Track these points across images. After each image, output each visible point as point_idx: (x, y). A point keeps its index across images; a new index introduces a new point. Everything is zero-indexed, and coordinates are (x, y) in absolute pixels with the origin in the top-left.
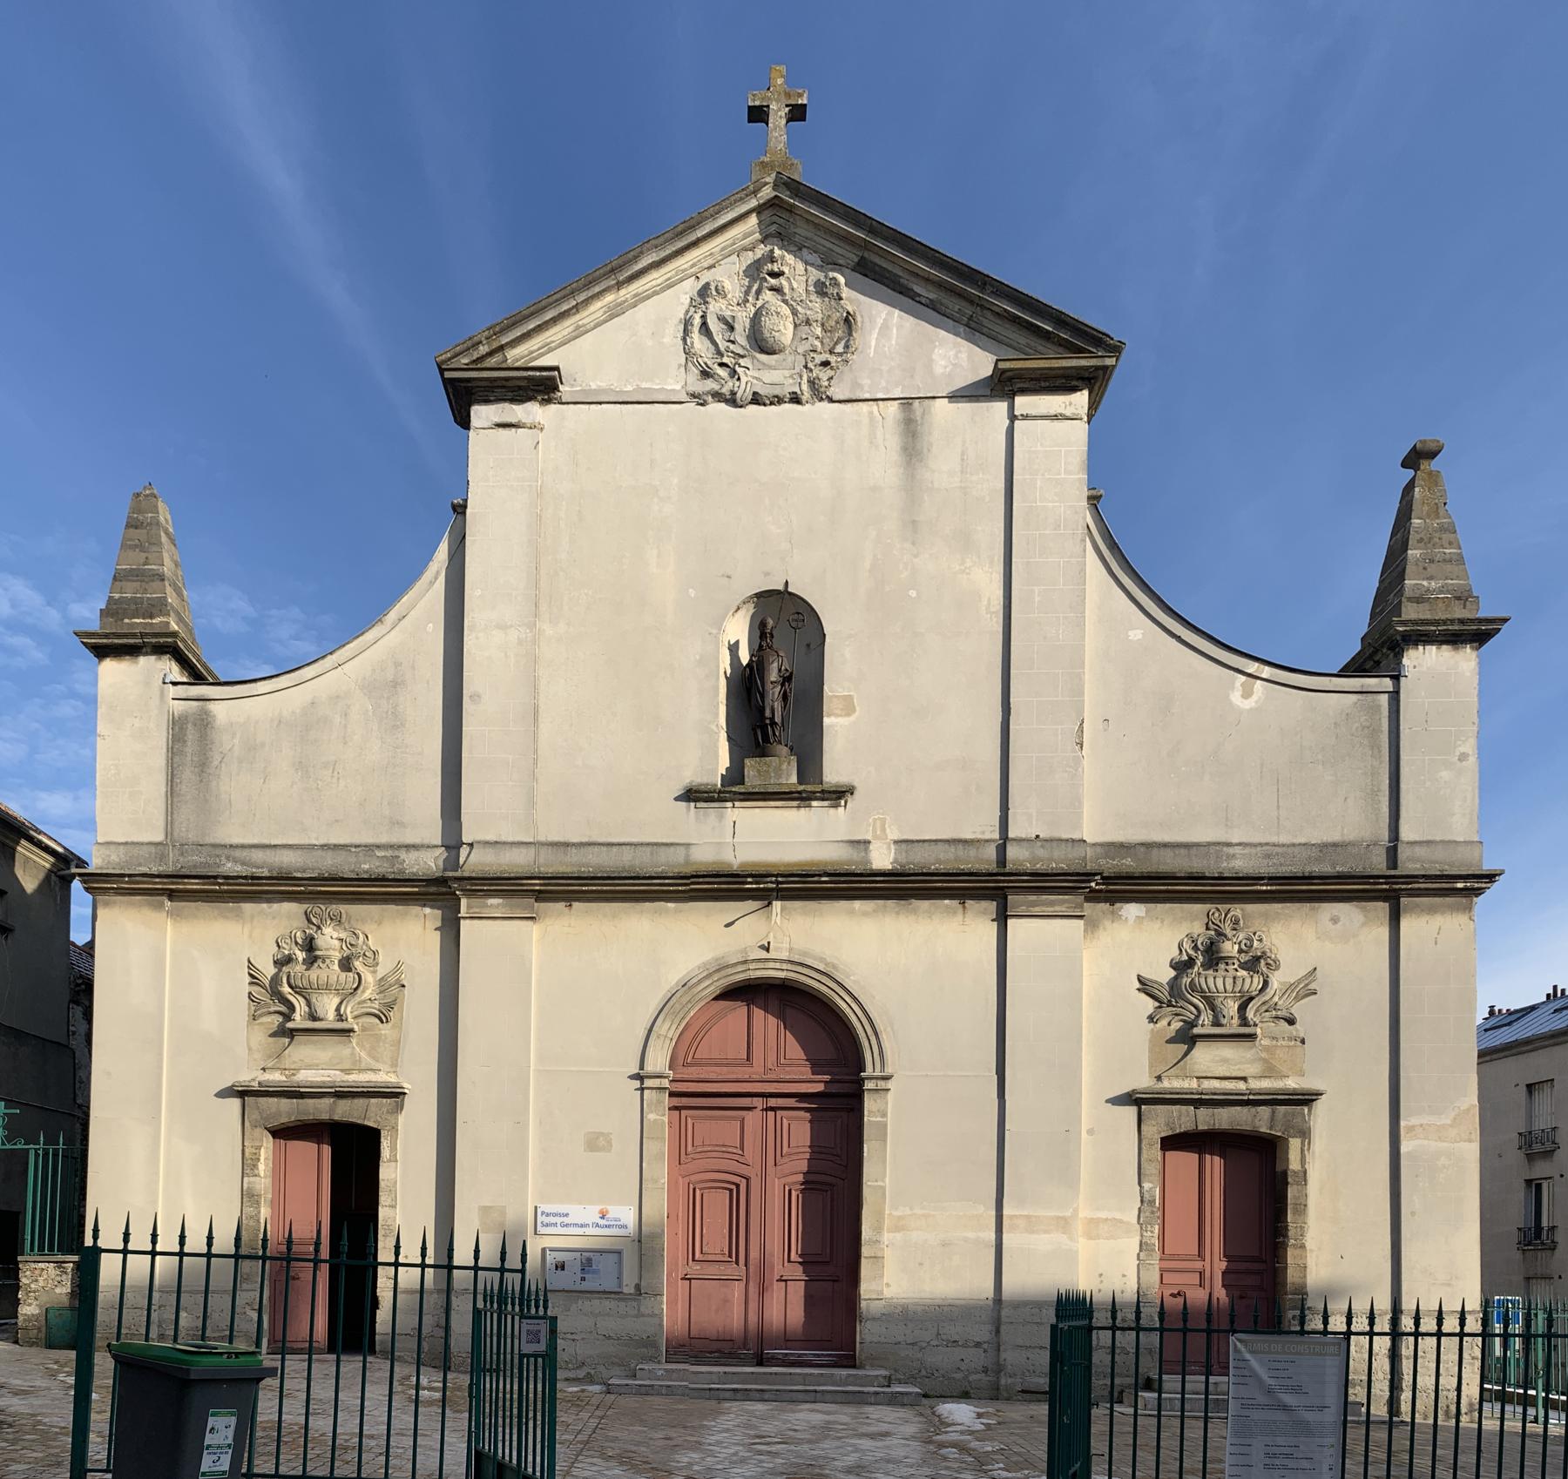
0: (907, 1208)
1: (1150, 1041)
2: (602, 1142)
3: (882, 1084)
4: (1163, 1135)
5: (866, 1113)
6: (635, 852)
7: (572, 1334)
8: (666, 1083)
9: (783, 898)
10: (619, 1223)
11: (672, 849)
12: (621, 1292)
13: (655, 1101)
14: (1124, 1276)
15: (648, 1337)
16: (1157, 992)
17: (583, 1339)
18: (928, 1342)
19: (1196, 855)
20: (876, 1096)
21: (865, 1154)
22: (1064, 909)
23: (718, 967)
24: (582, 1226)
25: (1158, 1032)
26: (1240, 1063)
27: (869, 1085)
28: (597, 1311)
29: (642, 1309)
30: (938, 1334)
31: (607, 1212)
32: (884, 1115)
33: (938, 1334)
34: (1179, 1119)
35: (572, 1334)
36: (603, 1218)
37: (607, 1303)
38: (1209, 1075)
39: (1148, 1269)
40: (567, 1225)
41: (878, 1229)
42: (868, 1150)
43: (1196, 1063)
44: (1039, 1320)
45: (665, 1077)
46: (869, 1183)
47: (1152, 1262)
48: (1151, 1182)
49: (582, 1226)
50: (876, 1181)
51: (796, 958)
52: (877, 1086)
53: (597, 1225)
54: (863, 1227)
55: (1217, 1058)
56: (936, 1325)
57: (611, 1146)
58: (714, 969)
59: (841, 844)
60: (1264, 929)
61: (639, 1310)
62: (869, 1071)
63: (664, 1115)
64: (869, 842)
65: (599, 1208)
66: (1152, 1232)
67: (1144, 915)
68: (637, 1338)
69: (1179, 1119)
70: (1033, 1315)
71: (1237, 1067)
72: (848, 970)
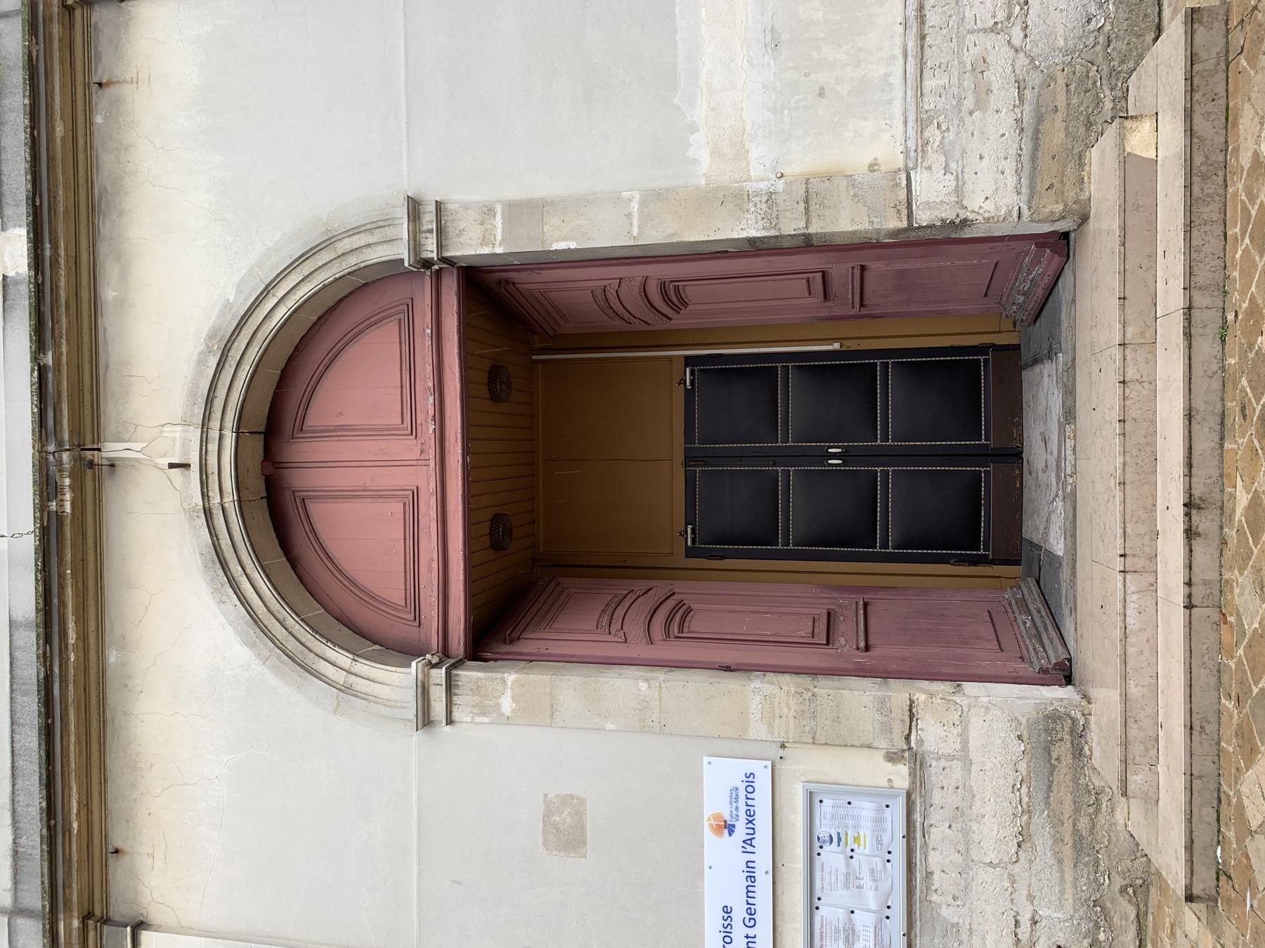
0: (692, 139)
2: (564, 818)
3: (428, 220)
5: (486, 250)
6: (24, 725)
7: (1017, 924)
8: (439, 675)
9: (97, 438)
10: (742, 793)
11: (17, 654)
12: (909, 795)
13: (476, 699)
15: (1019, 737)
17: (1031, 898)
18: (1016, 51)
20: (451, 232)
21: (573, 245)
23: (218, 565)
24: (751, 878)
27: (430, 249)
28: (958, 859)
29: (946, 749)
30: (994, 29)
31: (717, 817)
32: (489, 211)
33: (994, 29)
35: (1017, 924)
36: (731, 829)
37: (936, 835)
40: (751, 912)
41: (738, 199)
42: (566, 239)
45: (427, 676)
46: (635, 232)
49: (751, 878)
50: (629, 215)
51: (199, 411)
52: (431, 231)
53: (749, 842)
54: (735, 236)
56: (970, 38)
57: (572, 796)
58: (221, 573)
59: (9, 331)
61: (950, 758)
62: (401, 252)
63: (504, 681)
64: (5, 277)
65: (708, 834)
68: (1023, 766)
72: (219, 306)
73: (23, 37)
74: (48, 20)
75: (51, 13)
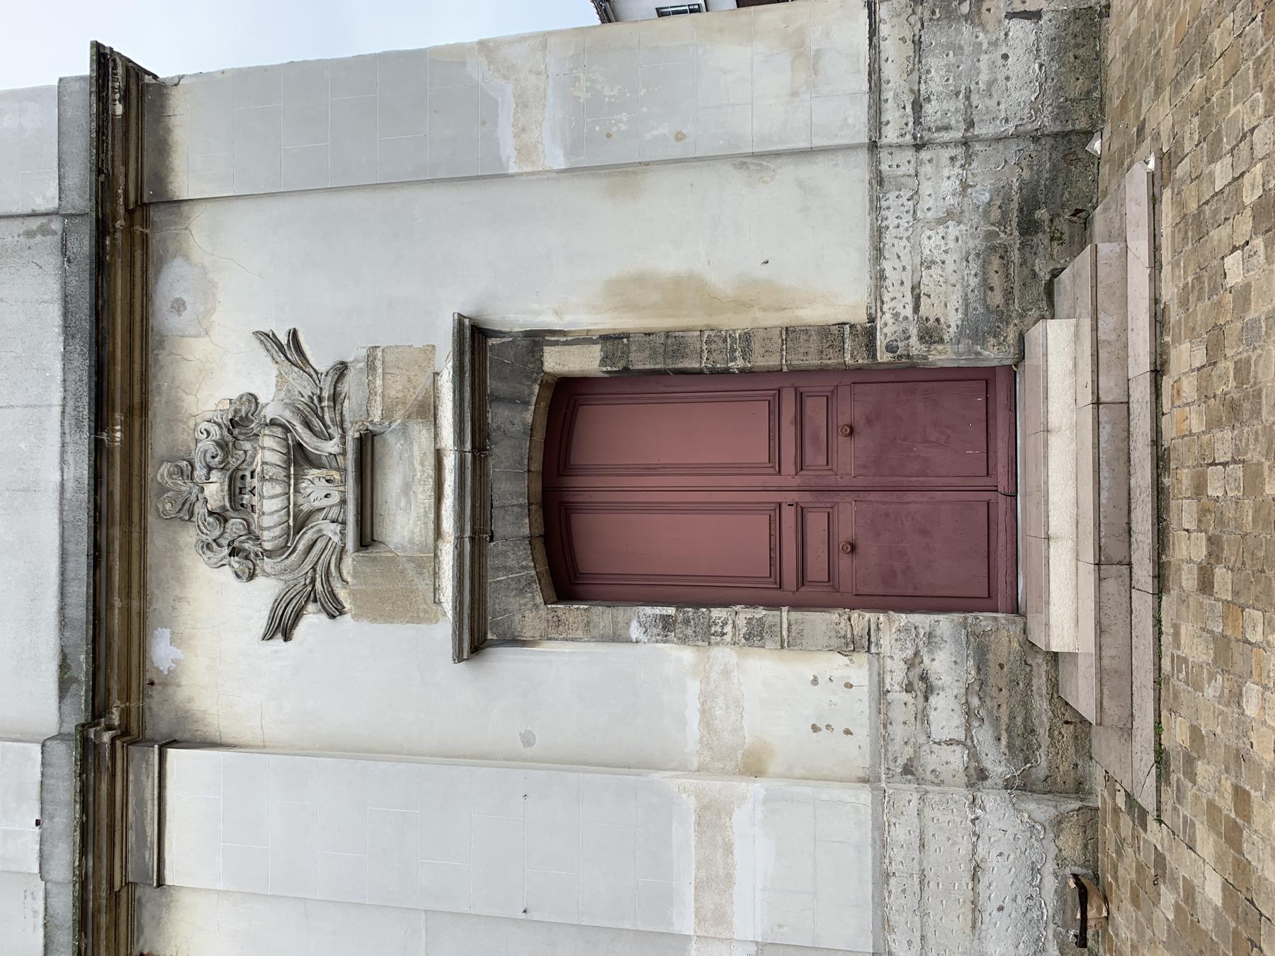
1: (374, 620)
4: (539, 600)
14: (815, 681)
16: (289, 609)
19: (77, 544)
22: (150, 783)
25: (359, 607)
26: (411, 463)
34: (509, 570)
38: (432, 516)
39: (801, 633)
43: (411, 541)
44: (916, 879)
47: (785, 626)
48: (628, 624)
55: (403, 504)
60: (192, 423)
66: (725, 624)
67: (169, 630)
69: (509, 570)
70: (904, 891)
71: (418, 467)
73: (74, 936)
74: (97, 911)
75: (100, 905)
